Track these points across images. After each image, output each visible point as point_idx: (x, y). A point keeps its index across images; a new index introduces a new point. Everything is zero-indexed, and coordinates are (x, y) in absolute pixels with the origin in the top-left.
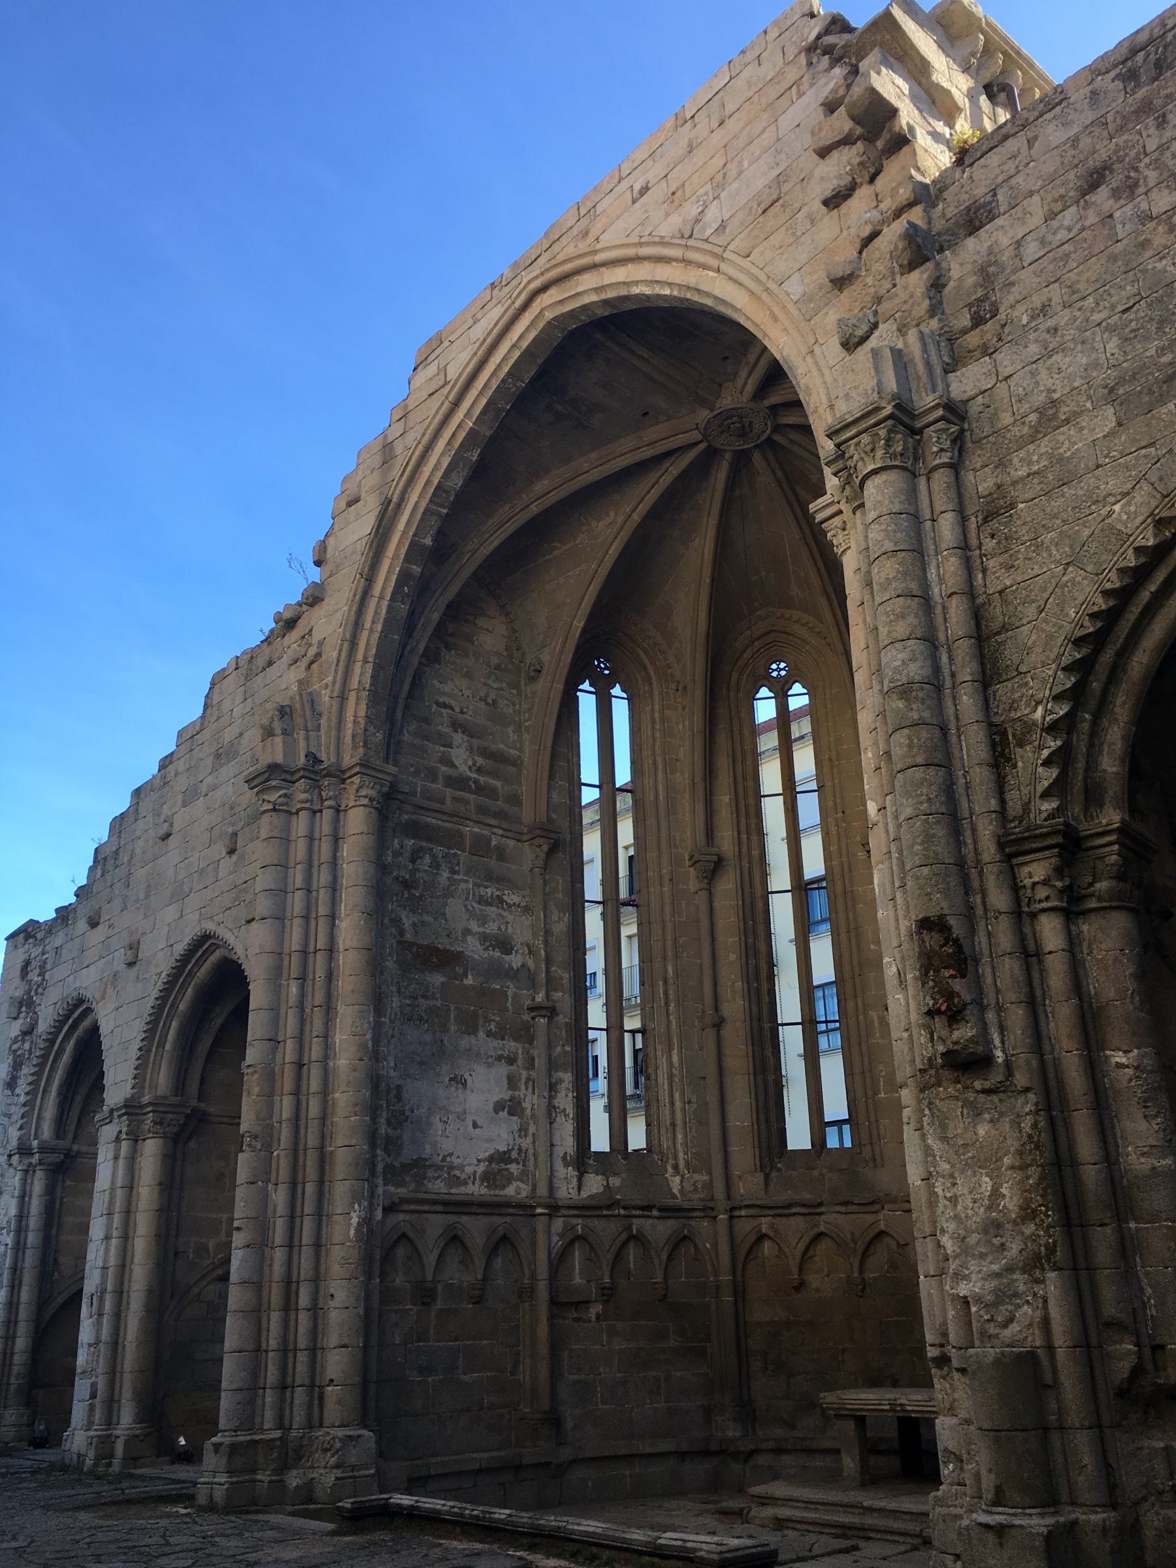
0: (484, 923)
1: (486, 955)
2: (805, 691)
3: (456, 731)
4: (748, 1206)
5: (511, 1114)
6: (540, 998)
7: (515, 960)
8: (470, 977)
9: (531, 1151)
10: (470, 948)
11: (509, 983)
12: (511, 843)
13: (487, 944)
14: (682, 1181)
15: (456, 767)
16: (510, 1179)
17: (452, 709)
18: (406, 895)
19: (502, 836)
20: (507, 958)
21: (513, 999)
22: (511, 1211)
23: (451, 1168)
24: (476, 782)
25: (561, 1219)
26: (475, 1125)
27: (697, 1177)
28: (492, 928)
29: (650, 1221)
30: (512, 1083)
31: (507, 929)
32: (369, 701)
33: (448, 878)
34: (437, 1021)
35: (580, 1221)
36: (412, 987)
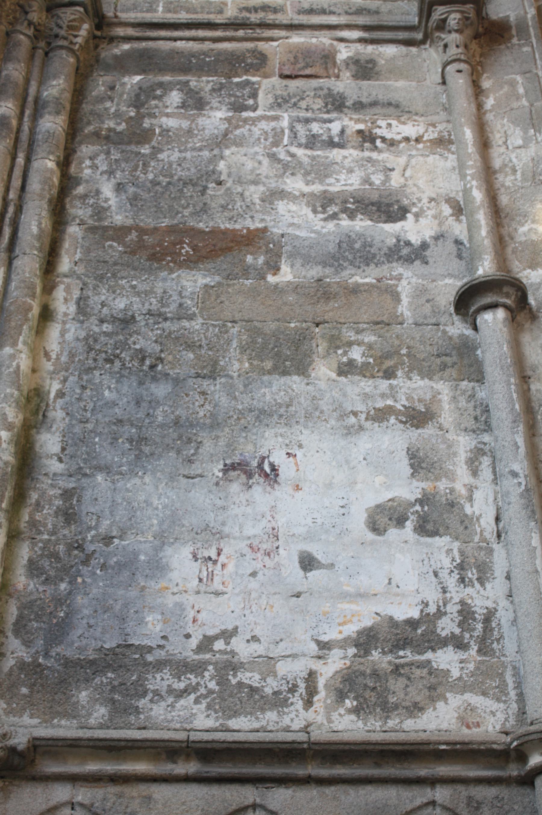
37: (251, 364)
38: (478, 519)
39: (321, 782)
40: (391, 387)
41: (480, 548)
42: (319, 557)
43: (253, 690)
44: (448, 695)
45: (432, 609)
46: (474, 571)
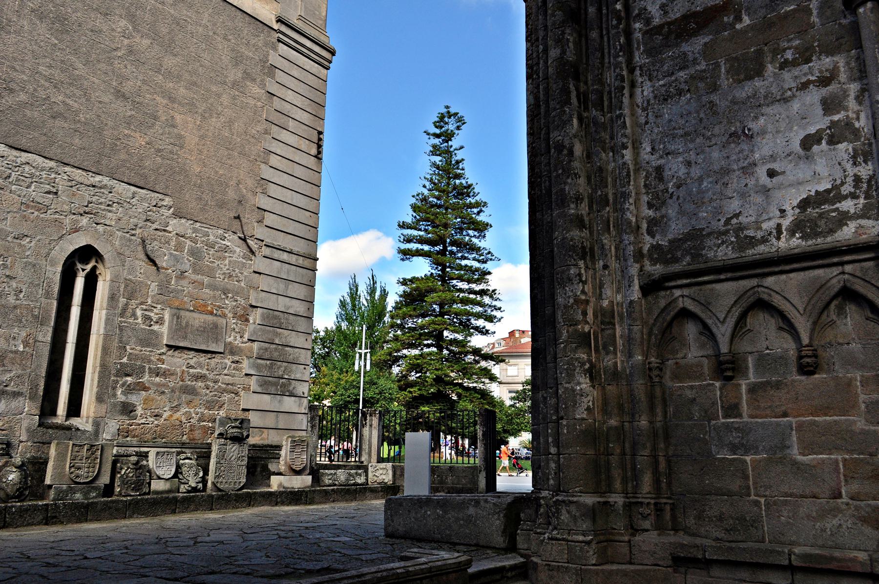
23: (741, 228)
30: (829, 106)
37: (733, 79)
38: (863, 128)
41: (865, 144)
42: (777, 169)
44: (848, 222)
45: (838, 182)
46: (862, 157)
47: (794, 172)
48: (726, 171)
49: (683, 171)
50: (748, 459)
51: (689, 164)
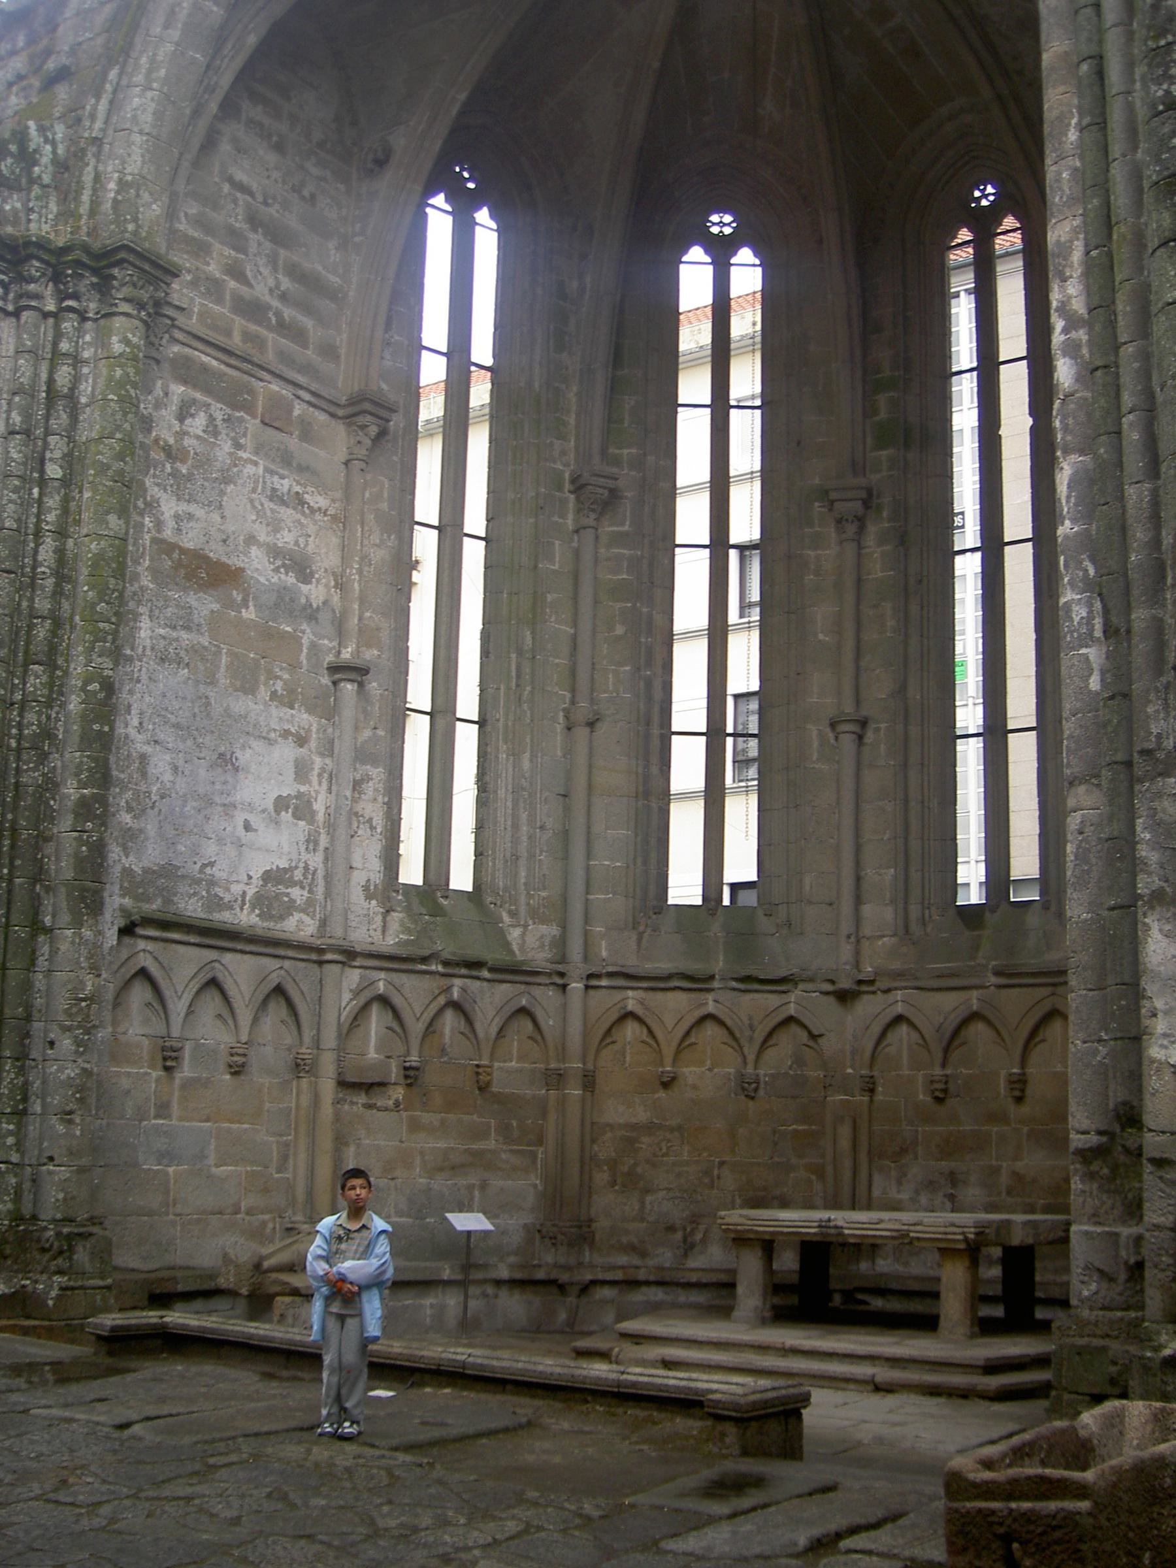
0: (276, 530)
1: (275, 580)
2: (757, 262)
3: (255, 231)
4: (611, 975)
5: (297, 816)
6: (347, 654)
7: (315, 592)
8: (252, 608)
9: (321, 873)
10: (255, 564)
11: (304, 626)
12: (322, 417)
13: (279, 563)
14: (523, 935)
15: (250, 286)
16: (290, 907)
17: (251, 194)
18: (168, 469)
19: (309, 403)
20: (305, 588)
21: (309, 649)
22: (290, 953)
23: (212, 883)
24: (278, 314)
25: (358, 971)
26: (247, 827)
27: (544, 929)
28: (286, 538)
29: (478, 983)
30: (301, 771)
31: (307, 545)
32: (148, 151)
33: (231, 454)
34: (201, 667)
35: (382, 975)
36: (170, 611)
39: (242, 952)
40: (292, 715)
43: (221, 899)
45: (293, 864)
47: (265, 836)
48: (210, 803)
49: (168, 777)
50: (171, 1170)
51: (175, 769)
